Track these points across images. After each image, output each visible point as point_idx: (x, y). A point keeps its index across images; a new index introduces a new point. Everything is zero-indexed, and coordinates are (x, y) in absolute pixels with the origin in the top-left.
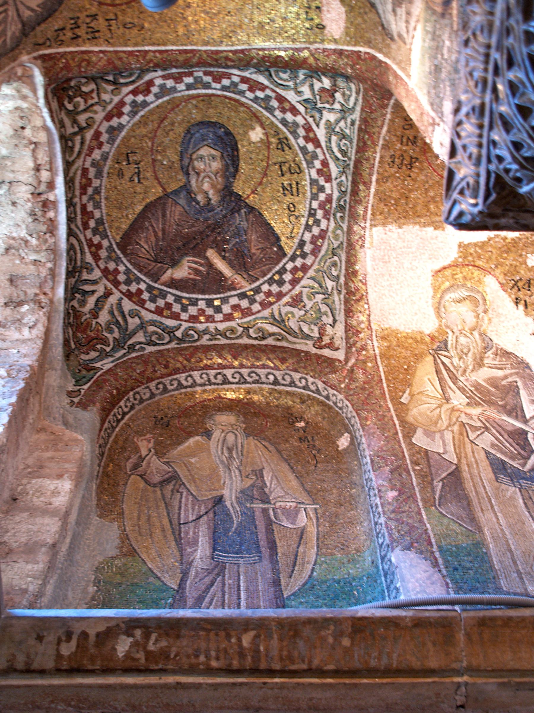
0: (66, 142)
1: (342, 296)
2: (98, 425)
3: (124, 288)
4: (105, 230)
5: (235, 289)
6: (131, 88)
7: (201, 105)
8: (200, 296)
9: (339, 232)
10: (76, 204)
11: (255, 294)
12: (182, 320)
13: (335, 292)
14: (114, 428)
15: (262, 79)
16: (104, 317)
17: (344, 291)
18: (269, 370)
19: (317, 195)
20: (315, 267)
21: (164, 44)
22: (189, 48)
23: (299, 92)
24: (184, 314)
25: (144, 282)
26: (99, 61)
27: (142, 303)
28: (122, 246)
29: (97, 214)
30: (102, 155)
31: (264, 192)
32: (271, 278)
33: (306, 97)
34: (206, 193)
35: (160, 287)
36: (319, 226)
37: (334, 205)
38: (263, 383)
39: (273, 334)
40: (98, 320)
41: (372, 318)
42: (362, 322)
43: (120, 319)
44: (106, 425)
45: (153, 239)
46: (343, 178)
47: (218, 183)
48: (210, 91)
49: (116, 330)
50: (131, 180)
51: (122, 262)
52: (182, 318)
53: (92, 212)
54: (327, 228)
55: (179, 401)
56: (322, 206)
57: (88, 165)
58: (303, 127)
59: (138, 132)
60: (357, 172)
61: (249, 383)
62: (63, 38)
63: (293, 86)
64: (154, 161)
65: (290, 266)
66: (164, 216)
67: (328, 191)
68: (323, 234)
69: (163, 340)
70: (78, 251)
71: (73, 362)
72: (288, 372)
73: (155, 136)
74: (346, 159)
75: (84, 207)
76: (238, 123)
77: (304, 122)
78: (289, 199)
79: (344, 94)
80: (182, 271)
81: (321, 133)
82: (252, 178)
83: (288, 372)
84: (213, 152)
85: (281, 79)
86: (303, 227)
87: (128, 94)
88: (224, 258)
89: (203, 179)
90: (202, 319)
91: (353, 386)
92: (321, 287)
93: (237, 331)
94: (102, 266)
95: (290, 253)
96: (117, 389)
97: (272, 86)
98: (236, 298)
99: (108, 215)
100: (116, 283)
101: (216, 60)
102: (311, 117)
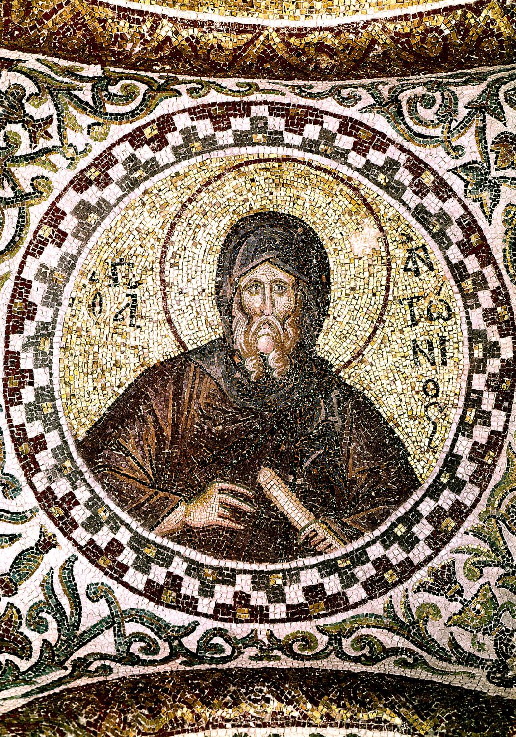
3: (81, 535)
6: (128, 128)
8: (242, 565)
11: (354, 565)
16: (28, 594)
19: (483, 361)
20: (481, 508)
23: (455, 149)
24: (206, 601)
25: (128, 526)
29: (41, 377)
30: (62, 259)
34: (263, 357)
35: (159, 540)
36: (487, 424)
39: (395, 651)
43: (65, 602)
47: (286, 337)
49: (53, 624)
51: (85, 480)
53: (31, 371)
57: (29, 273)
58: (459, 223)
65: (427, 507)
77: (462, 212)
80: (206, 512)
81: (495, 235)
84: (281, 275)
85: (420, 122)
86: (454, 427)
88: (292, 486)
94: (41, 488)
100: (67, 526)
102: (475, 201)
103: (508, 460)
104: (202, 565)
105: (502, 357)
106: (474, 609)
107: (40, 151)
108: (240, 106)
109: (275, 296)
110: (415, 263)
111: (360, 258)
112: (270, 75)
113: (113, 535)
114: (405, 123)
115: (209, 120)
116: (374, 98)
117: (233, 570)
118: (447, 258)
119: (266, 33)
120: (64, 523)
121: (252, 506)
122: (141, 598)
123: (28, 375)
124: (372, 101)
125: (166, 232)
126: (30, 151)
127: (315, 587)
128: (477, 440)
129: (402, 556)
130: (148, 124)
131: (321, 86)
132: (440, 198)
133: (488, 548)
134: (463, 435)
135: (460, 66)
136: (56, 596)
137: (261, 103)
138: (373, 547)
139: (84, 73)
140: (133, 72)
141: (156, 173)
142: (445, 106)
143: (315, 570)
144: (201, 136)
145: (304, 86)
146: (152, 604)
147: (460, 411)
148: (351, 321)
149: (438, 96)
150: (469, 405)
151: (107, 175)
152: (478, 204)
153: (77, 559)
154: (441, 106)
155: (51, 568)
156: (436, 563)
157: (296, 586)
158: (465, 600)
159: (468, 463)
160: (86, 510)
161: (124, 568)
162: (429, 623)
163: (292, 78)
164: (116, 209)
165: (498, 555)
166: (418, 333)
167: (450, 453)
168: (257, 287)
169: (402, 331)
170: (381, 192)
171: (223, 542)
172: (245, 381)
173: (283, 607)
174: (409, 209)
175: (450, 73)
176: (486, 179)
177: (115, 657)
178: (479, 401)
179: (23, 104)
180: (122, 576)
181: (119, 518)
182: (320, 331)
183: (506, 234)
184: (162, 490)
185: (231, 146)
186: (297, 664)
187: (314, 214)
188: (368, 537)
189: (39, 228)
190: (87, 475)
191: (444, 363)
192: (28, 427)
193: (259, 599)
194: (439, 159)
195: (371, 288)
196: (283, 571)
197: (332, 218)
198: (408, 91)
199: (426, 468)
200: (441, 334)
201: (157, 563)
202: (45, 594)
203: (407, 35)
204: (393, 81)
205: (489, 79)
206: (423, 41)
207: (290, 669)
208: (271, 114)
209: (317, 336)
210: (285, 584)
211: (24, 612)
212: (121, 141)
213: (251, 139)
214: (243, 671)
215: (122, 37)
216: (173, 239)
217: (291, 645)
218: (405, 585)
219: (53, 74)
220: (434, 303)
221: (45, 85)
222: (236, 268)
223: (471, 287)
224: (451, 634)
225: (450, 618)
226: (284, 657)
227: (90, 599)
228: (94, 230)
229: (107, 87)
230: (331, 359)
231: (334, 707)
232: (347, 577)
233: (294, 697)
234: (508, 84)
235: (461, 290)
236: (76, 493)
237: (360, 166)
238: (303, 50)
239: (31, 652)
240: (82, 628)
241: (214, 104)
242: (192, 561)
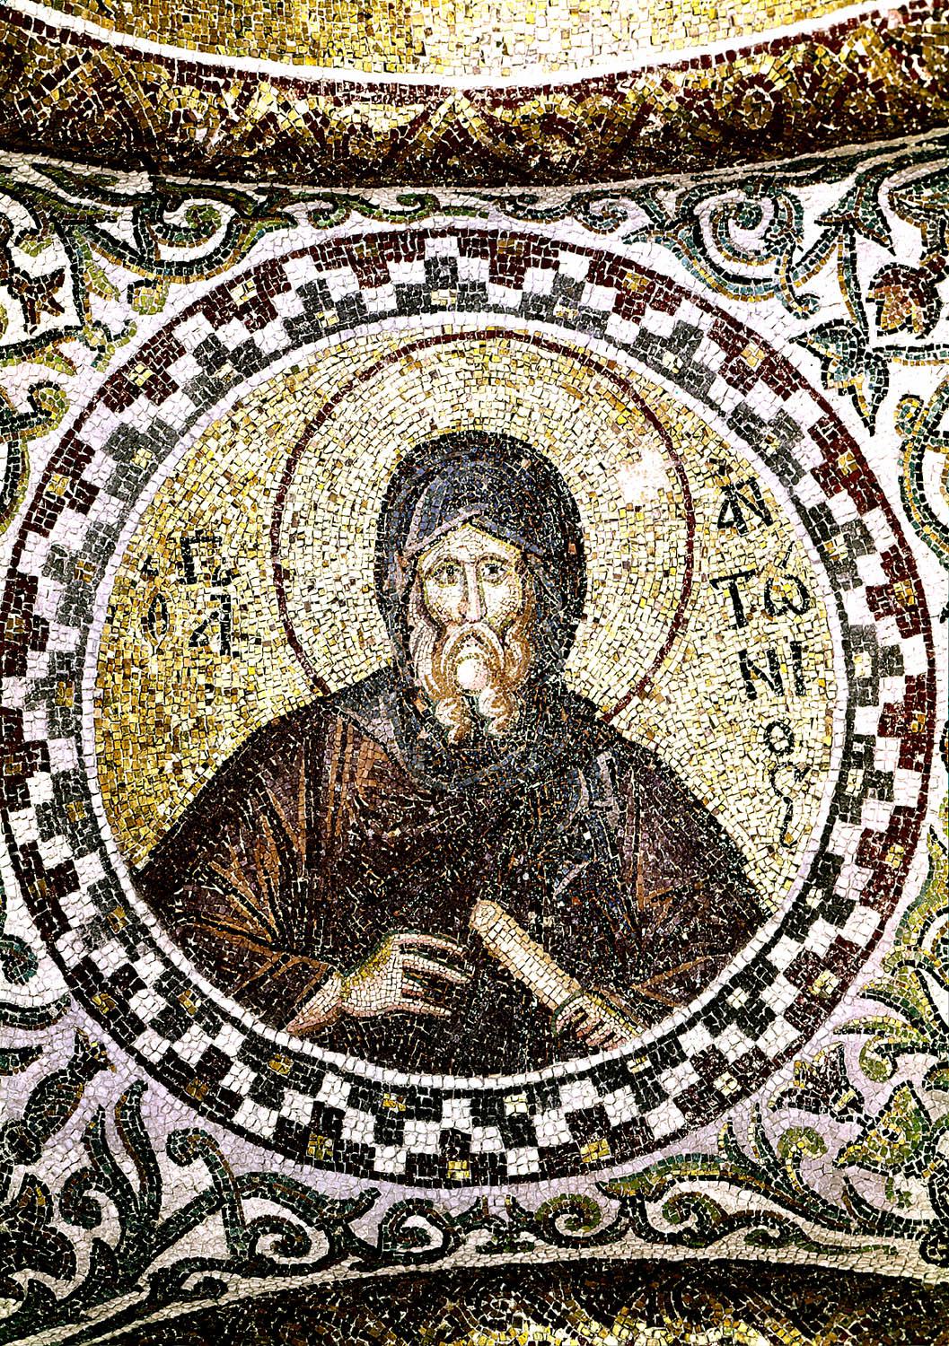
3: (152, 1044)
6: (202, 288)
8: (450, 1082)
11: (658, 1067)
12: (376, 1176)
16: (60, 1160)
19: (872, 682)
20: (884, 949)
24: (390, 1151)
25: (236, 1023)
28: (156, 885)
29: (62, 755)
30: (91, 536)
35: (295, 1045)
36: (885, 795)
39: (745, 1218)
40: (39, 1170)
43: (128, 1167)
45: (273, 861)
47: (510, 659)
51: (152, 943)
53: (43, 744)
54: (923, 801)
57: (32, 563)
63: (779, 280)
65: (784, 954)
66: (316, 776)
67: (915, 663)
77: (820, 413)
80: (379, 990)
81: (883, 453)
84: (494, 547)
85: (736, 254)
86: (826, 804)
88: (538, 934)
89: (456, 649)
90: (459, 1170)
93: (597, 1210)
94: (72, 960)
100: (126, 1028)
102: (841, 392)
103: (930, 858)
104: (377, 1085)
105: (907, 673)
106: (885, 1132)
107: (42, 336)
108: (404, 239)
109: (486, 586)
110: (737, 511)
111: (638, 509)
112: (460, 180)
113: (209, 1041)
114: (708, 259)
115: (349, 269)
116: (650, 215)
117: (436, 1092)
118: (796, 501)
119: (449, 101)
120: (119, 1024)
123: (38, 751)
124: (647, 221)
125: (279, 477)
126: (25, 337)
127: (589, 1111)
128: (871, 826)
130: (238, 279)
131: (553, 197)
132: (778, 391)
133: (903, 1018)
134: (844, 819)
135: (808, 146)
136: (111, 1158)
137: (443, 234)
138: (690, 1033)
139: (120, 189)
140: (209, 183)
141: (256, 369)
142: (780, 223)
143: (588, 1082)
144: (336, 298)
145: (522, 197)
146: (290, 1162)
147: (835, 776)
148: (626, 624)
149: (766, 204)
150: (850, 765)
151: (166, 377)
152: (849, 397)
153: (145, 1088)
154: (772, 223)
155: (100, 1108)
156: (808, 1053)
157: (553, 1113)
158: (867, 1118)
159: (857, 868)
160: (158, 997)
161: (234, 1100)
162: (803, 1164)
163: (498, 183)
164: (186, 440)
165: (923, 1032)
166: (752, 640)
167: (822, 854)
169: (720, 636)
170: (670, 385)
171: (413, 1041)
172: (438, 745)
173: (533, 1154)
174: (722, 414)
175: (787, 161)
176: (861, 352)
177: (230, 1263)
178: (869, 756)
179: (8, 251)
180: (232, 1115)
181: (219, 1010)
182: (569, 645)
183: (903, 449)
185: (393, 314)
186: (565, 1254)
187: (549, 431)
188: (680, 1016)
189: (46, 478)
190: (155, 932)
192: (43, 849)
193: (487, 1140)
194: (772, 320)
195: (659, 561)
196: (527, 1087)
197: (583, 437)
198: (712, 199)
199: (778, 883)
200: (791, 639)
201: (296, 1087)
202: (91, 1156)
203: (706, 94)
204: (684, 181)
205: (860, 169)
206: (736, 103)
207: (553, 1265)
208: (462, 253)
209: (567, 654)
210: (533, 1111)
211: (55, 1190)
212: (189, 312)
213: (428, 299)
214: (465, 1275)
215: (188, 116)
216: (292, 489)
217: (552, 1221)
218: (754, 1097)
219: (61, 193)
221: (48, 215)
222: (412, 536)
223: (844, 549)
224: (847, 1180)
225: (842, 1151)
226: (540, 1243)
227: (175, 1160)
228: (147, 479)
229: (161, 213)
230: (594, 696)
231: (642, 1326)
232: (647, 1091)
233: (565, 1312)
234: (895, 177)
235: (824, 557)
236: (137, 965)
237: (630, 340)
238: (518, 129)
239: (74, 1263)
240: (165, 1215)
241: (357, 238)
242: (359, 1080)
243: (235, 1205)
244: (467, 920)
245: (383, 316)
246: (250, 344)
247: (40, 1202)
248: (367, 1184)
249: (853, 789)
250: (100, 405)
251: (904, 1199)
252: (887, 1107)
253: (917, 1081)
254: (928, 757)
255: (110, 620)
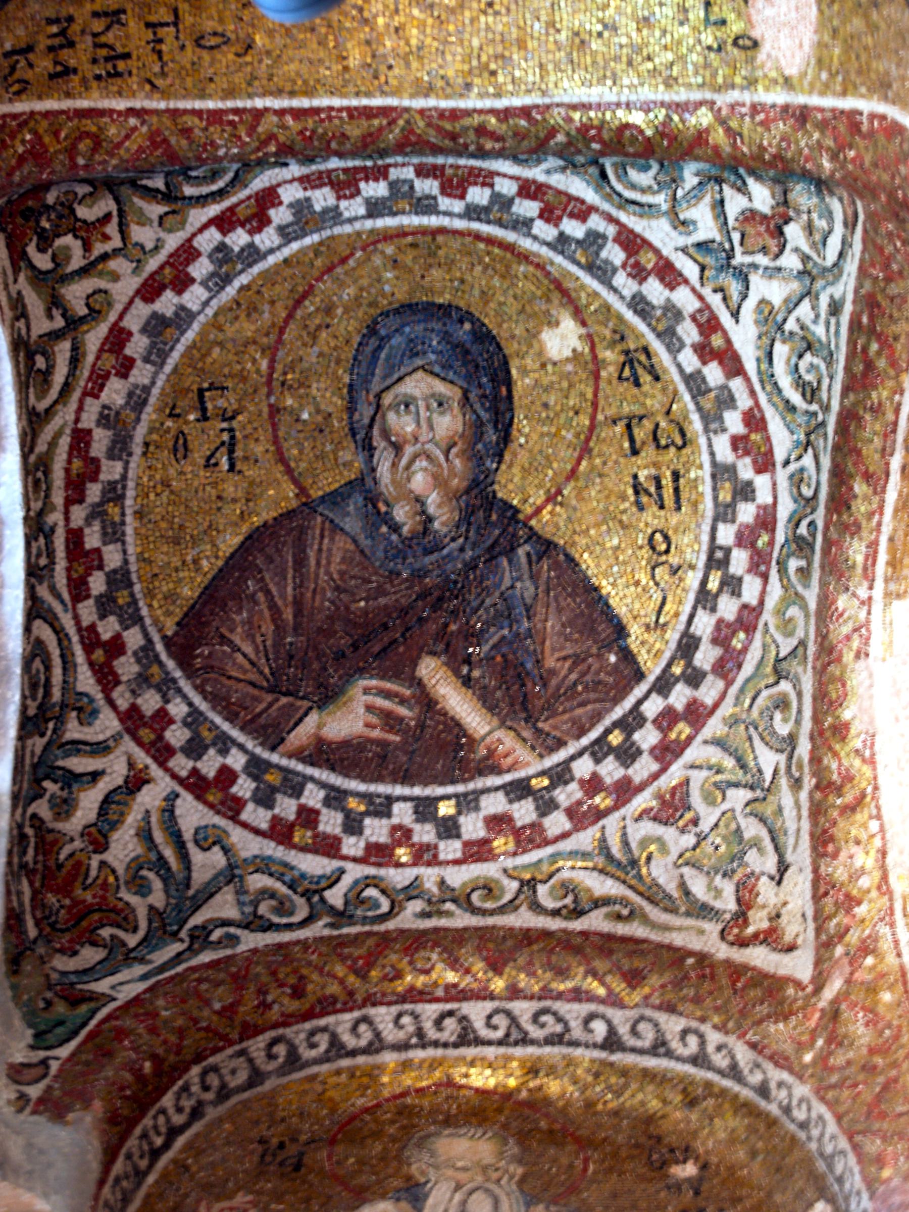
0: (30, 357)
1: (804, 795)
2: (95, 1166)
3: (182, 764)
4: (134, 602)
5: (497, 770)
6: (214, 210)
7: (408, 259)
8: (399, 790)
9: (793, 611)
10: (52, 530)
11: (552, 786)
12: (345, 858)
13: (783, 781)
14: (140, 1175)
15: (578, 187)
16: (123, 847)
17: (809, 782)
18: (592, 1007)
20: (727, 709)
21: (309, 93)
22: (377, 102)
23: (683, 223)
24: (352, 840)
25: (242, 747)
26: (127, 137)
27: (232, 808)
28: (183, 647)
29: (112, 557)
30: (130, 395)
31: (580, 498)
32: (601, 740)
33: (701, 235)
34: (419, 500)
35: (284, 762)
36: (736, 592)
37: (780, 537)
38: (575, 1044)
39: (605, 901)
40: (108, 857)
41: (889, 860)
42: (862, 871)
43: (169, 853)
44: (119, 1167)
45: (268, 628)
46: (808, 460)
47: (453, 473)
48: (433, 221)
50: (210, 463)
51: (179, 691)
52: (345, 851)
53: (98, 551)
54: (762, 602)
55: (331, 1093)
56: (745, 539)
57: (88, 420)
58: (694, 318)
59: (230, 331)
60: (846, 447)
61: (533, 1042)
62: (29, 75)
63: (665, 207)
64: (274, 410)
65: (653, 707)
66: (300, 562)
67: (764, 496)
68: (748, 619)
69: (291, 914)
70: (57, 661)
71: (31, 979)
72: (648, 1012)
73: (279, 341)
74: (814, 407)
75: (75, 537)
76: (512, 307)
77: (697, 305)
78: (652, 518)
79: (809, 228)
80: (349, 719)
81: (744, 336)
82: (547, 458)
83: (648, 1012)
84: (441, 387)
85: (633, 187)
86: (691, 597)
87: (202, 230)
88: (467, 682)
90: (403, 854)
91: (838, 1059)
92: (743, 766)
93: (503, 891)
94: (123, 704)
95: (654, 670)
96: (154, 1057)
97: (606, 206)
98: (500, 796)
99: (141, 558)
100: (162, 753)
101: (453, 137)
121: (410, 708)
122: (266, 842)
126: (83, 263)
129: (620, 773)
147: (700, 575)
151: (187, 274)
153: (177, 796)
157: (473, 815)
162: (653, 863)
167: (686, 634)
168: (407, 406)
170: (580, 273)
173: (457, 845)
174: (622, 297)
178: (725, 562)
184: (285, 694)
189: (98, 358)
191: (679, 508)
193: (425, 833)
196: (456, 796)
199: (653, 653)
210: (459, 813)
218: (623, 811)
220: (663, 424)
222: (376, 379)
226: (458, 912)
243: (241, 877)
244: (414, 670)
245: (356, 219)
246: (251, 245)
247: (111, 879)
248: (336, 864)
249: (713, 584)
250: (137, 300)
251: (718, 893)
252: (716, 825)
253: (739, 809)
254: (768, 568)
255: (145, 454)
